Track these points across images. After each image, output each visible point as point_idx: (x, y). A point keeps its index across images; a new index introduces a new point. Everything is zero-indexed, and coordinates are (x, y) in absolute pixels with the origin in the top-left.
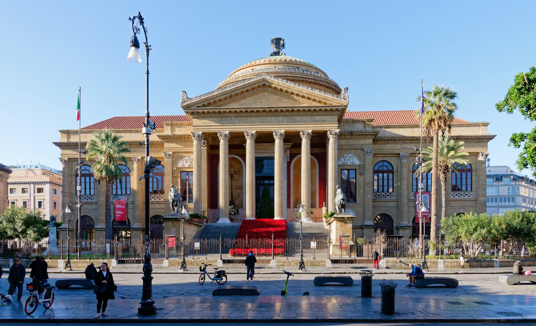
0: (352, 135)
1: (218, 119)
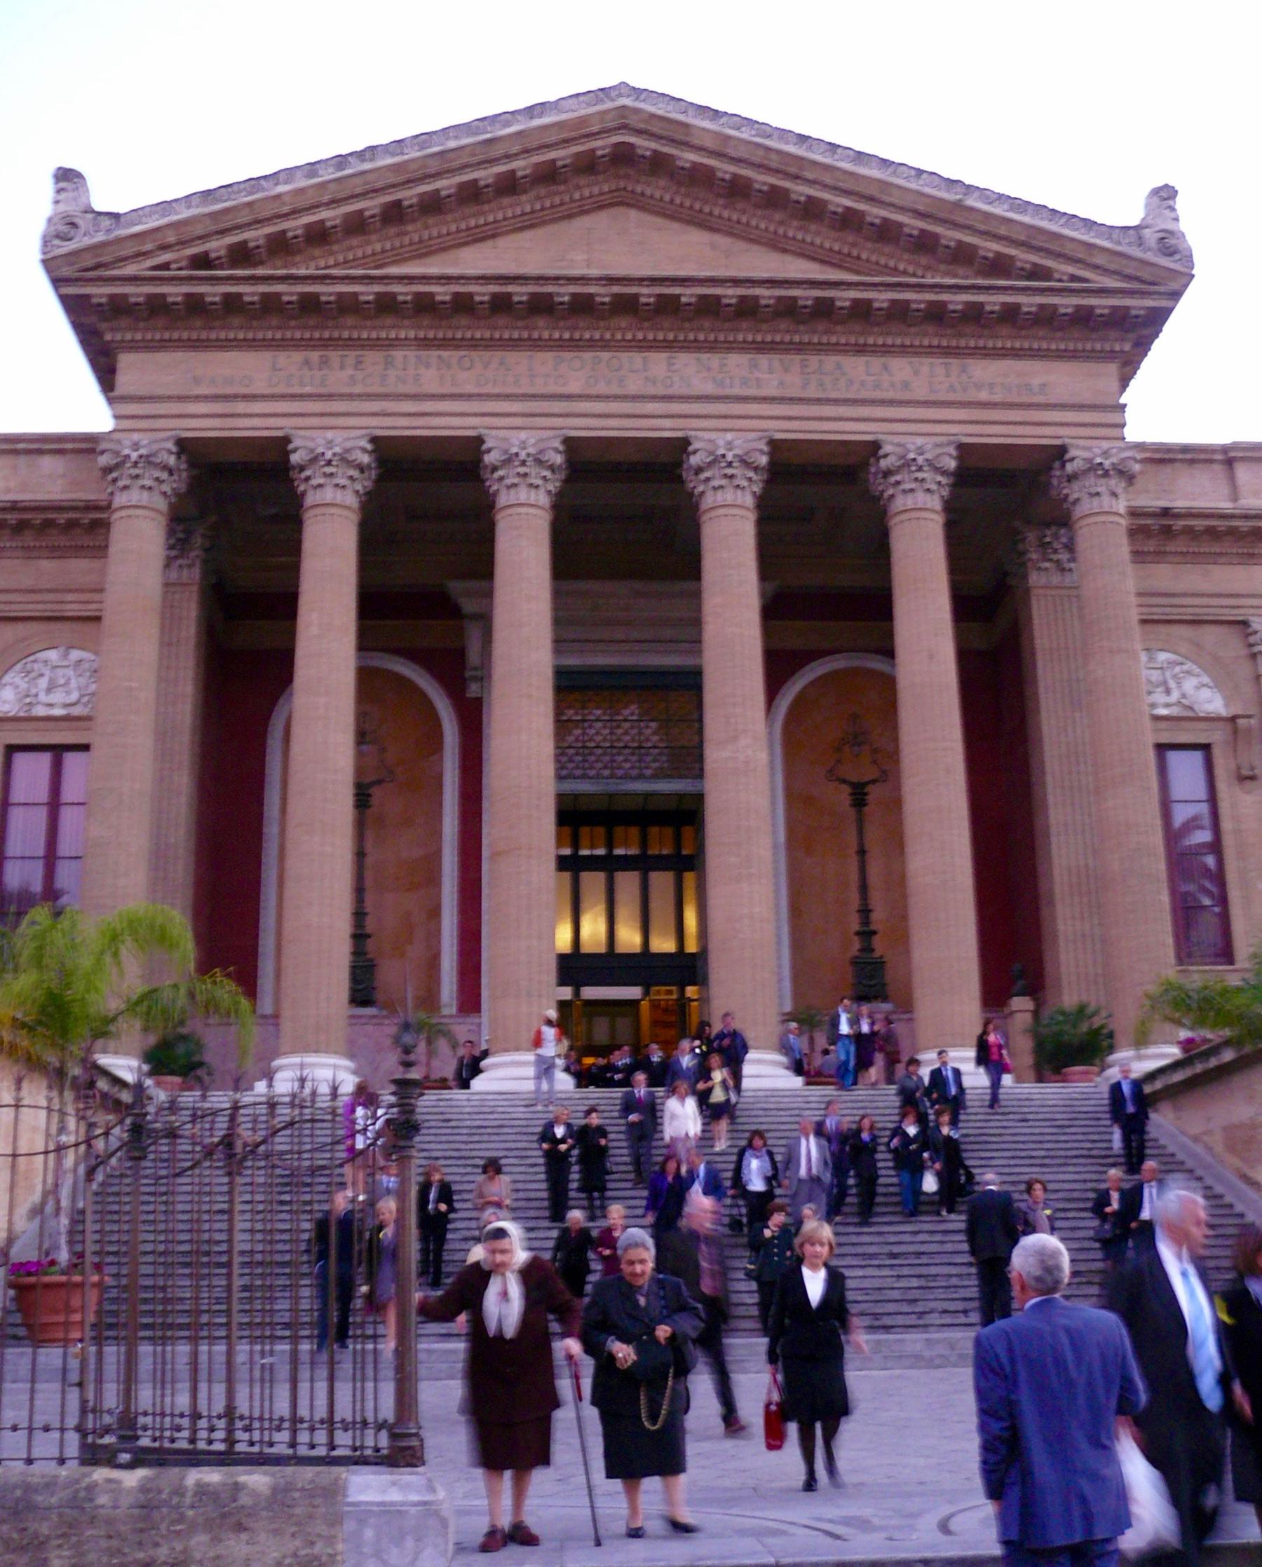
0: (1167, 532)
1: (297, 356)
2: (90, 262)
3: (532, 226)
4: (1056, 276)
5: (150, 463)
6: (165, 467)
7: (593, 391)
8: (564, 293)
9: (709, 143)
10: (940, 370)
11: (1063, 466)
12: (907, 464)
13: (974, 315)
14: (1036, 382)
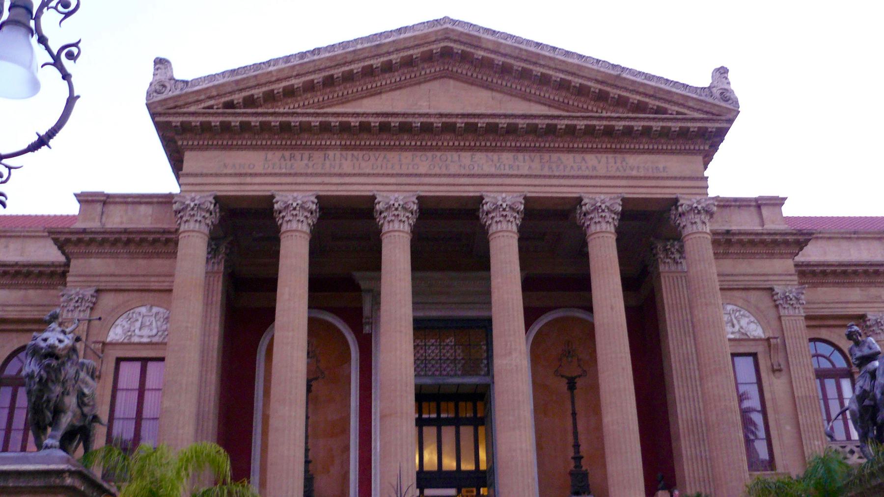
1: (278, 154)
2: (172, 105)
3: (400, 88)
4: (670, 112)
5: (201, 209)
6: (208, 211)
7: (433, 172)
8: (417, 122)
9: (490, 46)
10: (611, 160)
11: (677, 209)
12: (596, 209)
13: (628, 132)
14: (661, 166)
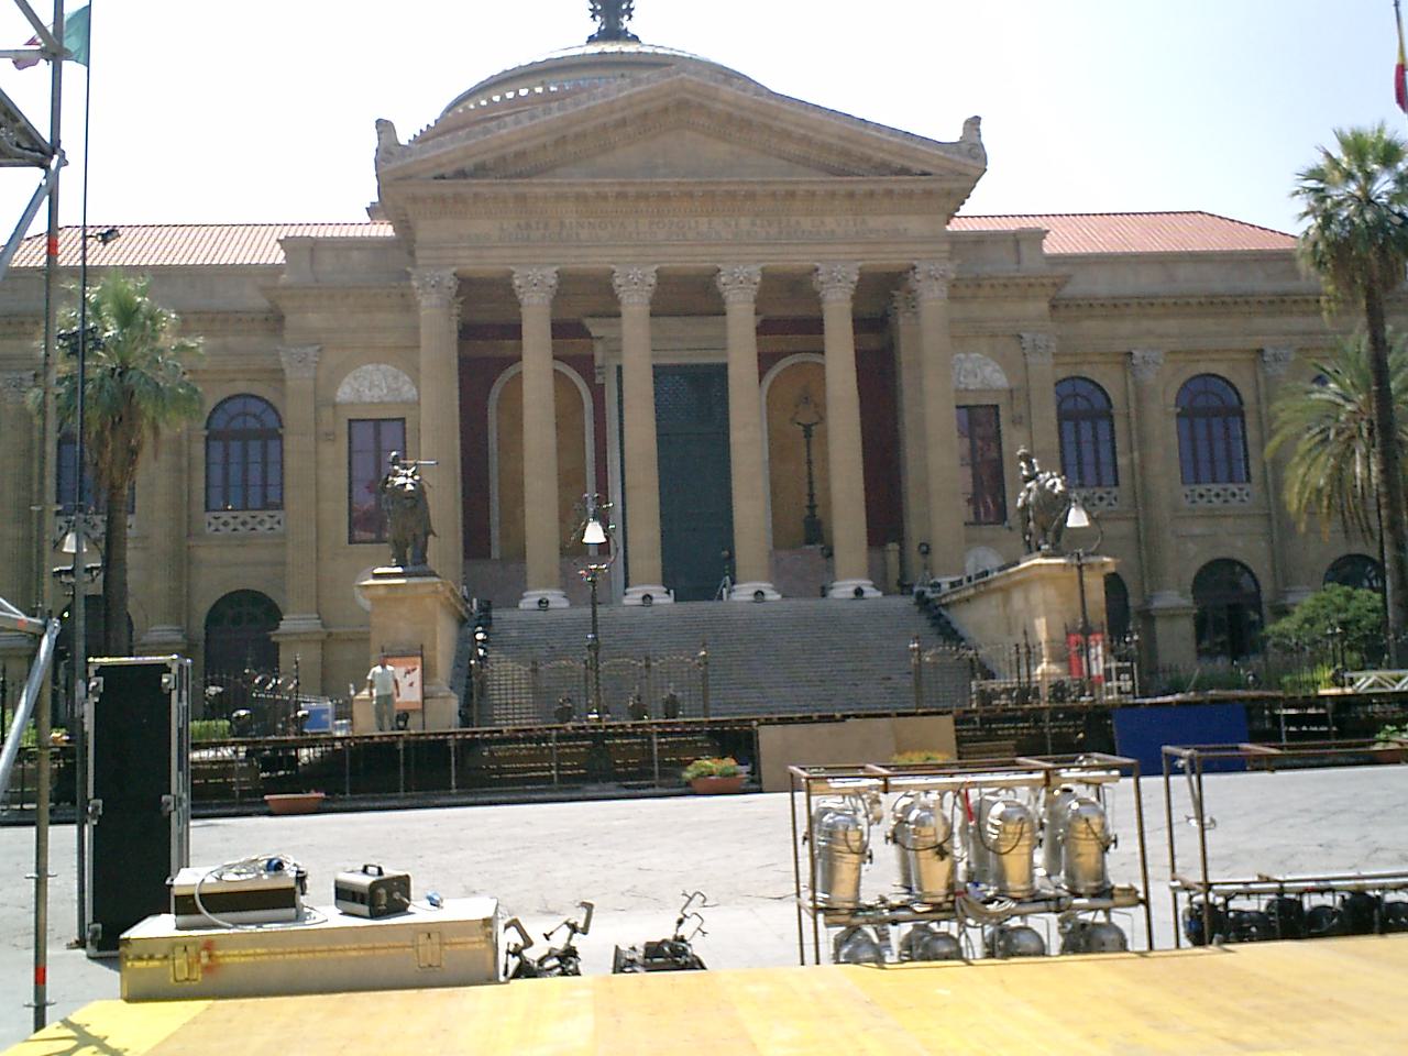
10: (851, 223)
